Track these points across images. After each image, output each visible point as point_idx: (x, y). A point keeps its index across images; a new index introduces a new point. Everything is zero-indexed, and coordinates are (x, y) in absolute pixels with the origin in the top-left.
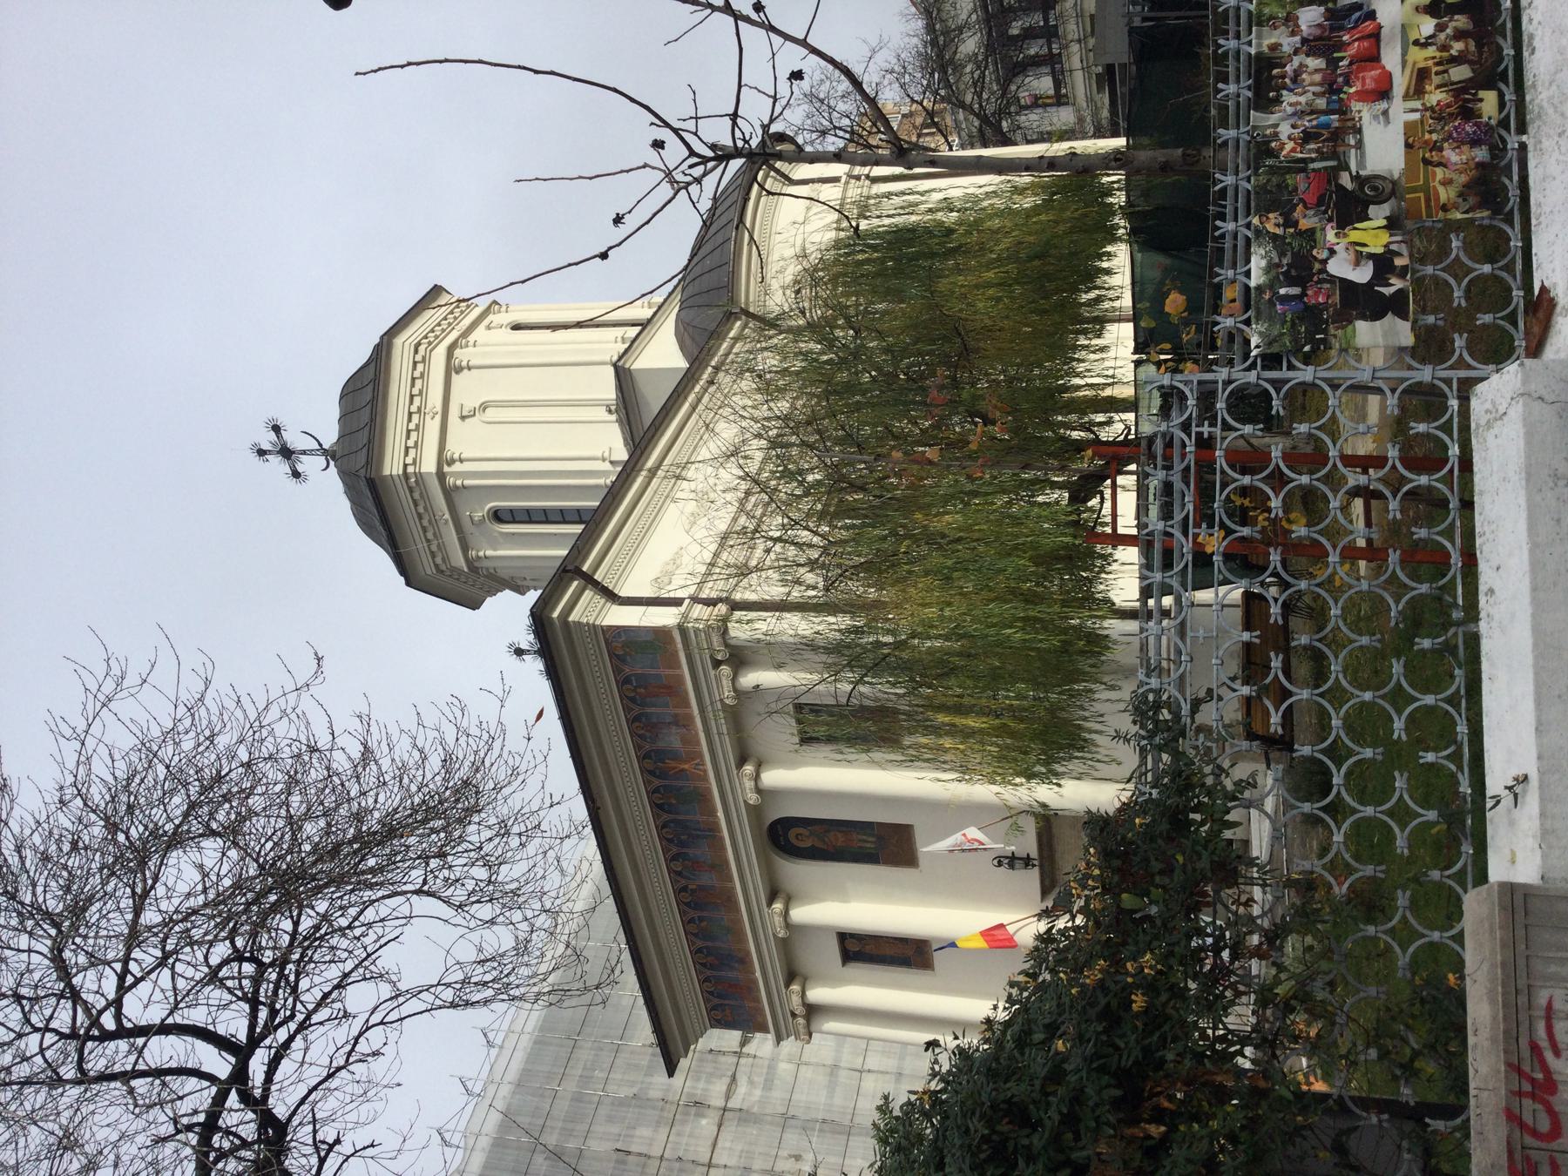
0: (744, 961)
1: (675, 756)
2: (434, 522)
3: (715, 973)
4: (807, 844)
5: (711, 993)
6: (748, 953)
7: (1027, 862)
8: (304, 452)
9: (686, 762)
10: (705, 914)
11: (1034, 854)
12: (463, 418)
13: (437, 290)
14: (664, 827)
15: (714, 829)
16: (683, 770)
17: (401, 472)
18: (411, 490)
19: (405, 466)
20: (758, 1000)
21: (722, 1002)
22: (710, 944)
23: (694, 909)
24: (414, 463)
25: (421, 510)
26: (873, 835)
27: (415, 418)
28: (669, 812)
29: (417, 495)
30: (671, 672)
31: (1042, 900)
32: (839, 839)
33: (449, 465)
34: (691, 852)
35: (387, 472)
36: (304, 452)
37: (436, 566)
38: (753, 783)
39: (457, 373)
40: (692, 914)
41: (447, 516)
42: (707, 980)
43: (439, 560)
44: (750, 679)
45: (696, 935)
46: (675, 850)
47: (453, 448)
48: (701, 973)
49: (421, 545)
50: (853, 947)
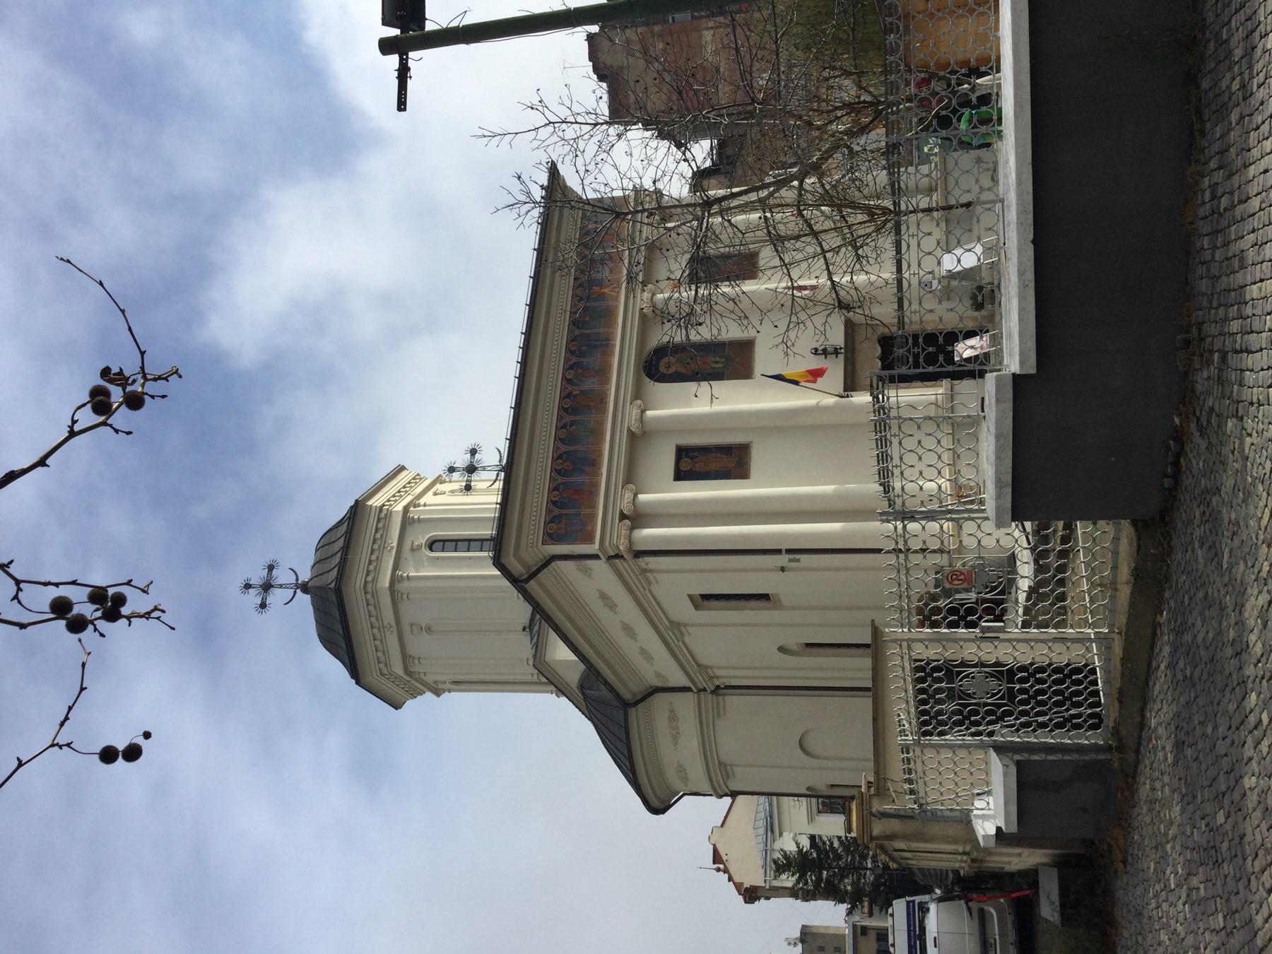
2: (383, 548)
4: (671, 370)
6: (600, 454)
7: (836, 352)
8: (281, 586)
9: (607, 286)
18: (379, 521)
19: (383, 505)
20: (593, 506)
22: (571, 448)
28: (578, 328)
29: (381, 525)
36: (281, 586)
37: (366, 582)
38: (650, 295)
40: (568, 419)
41: (395, 544)
46: (574, 360)
50: (685, 466)
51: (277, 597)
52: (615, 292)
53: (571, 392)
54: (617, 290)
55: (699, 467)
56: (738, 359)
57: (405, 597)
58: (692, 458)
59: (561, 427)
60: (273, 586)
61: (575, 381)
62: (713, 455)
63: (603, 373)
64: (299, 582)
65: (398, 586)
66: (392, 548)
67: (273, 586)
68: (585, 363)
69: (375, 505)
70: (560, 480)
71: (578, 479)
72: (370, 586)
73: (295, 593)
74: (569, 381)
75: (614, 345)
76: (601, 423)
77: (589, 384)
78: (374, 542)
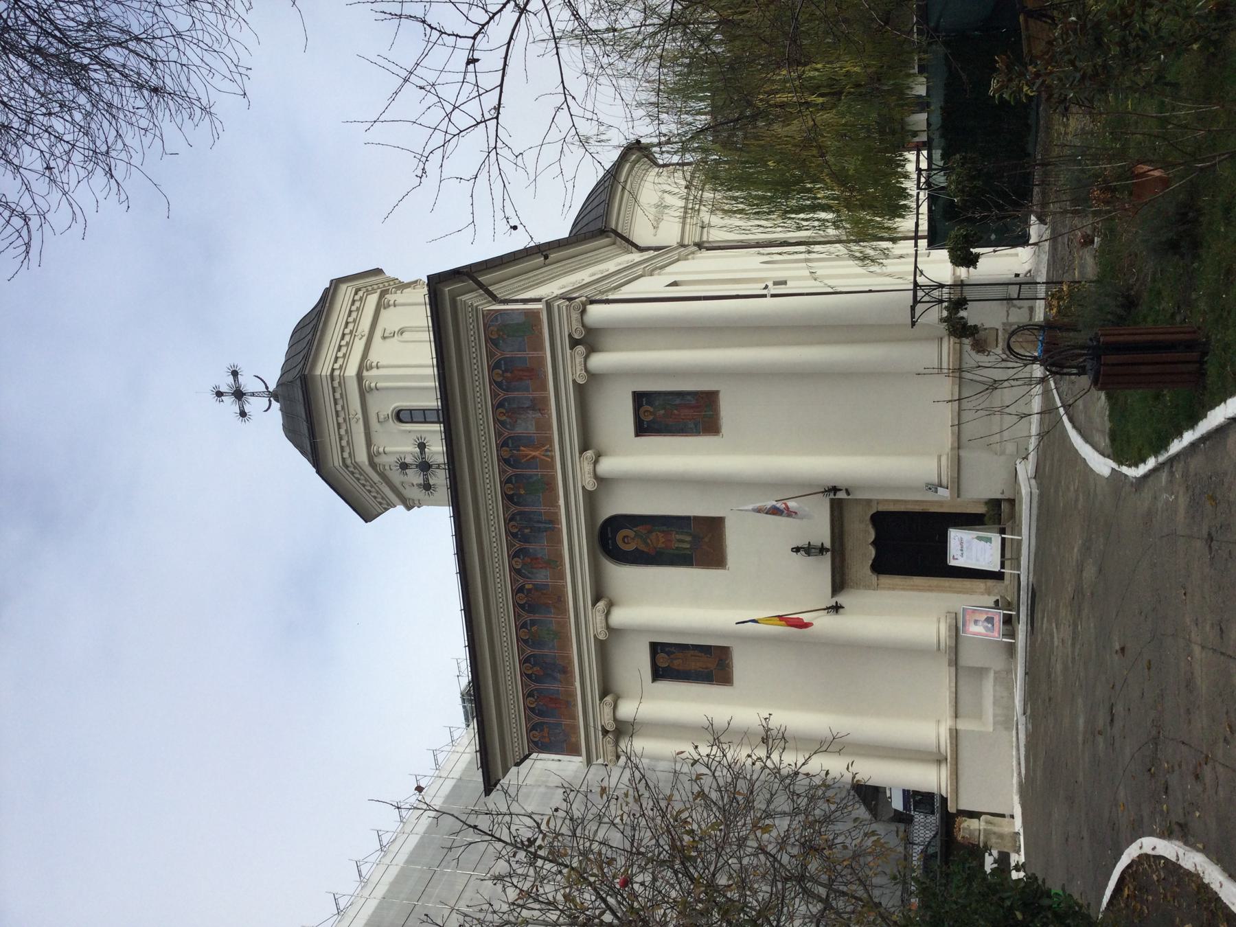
0: (566, 671)
1: (530, 442)
3: (539, 686)
4: (630, 547)
5: (532, 710)
6: (570, 661)
7: (822, 550)
8: (253, 394)
9: (537, 448)
10: (536, 617)
11: (828, 544)
12: (384, 338)
13: (378, 272)
14: (511, 520)
15: (553, 521)
16: (534, 457)
17: (329, 373)
19: (333, 370)
20: (574, 717)
21: (542, 720)
22: (537, 652)
23: (529, 612)
24: (341, 367)
25: (339, 408)
26: (690, 534)
27: (347, 338)
28: (515, 504)
30: (535, 354)
31: (832, 597)
32: (658, 540)
33: (367, 370)
34: (531, 547)
35: (318, 372)
36: (253, 394)
37: (344, 459)
38: (591, 467)
39: (385, 308)
40: (527, 617)
41: (360, 415)
42: (530, 695)
43: (346, 455)
44: (599, 361)
45: (525, 641)
46: (518, 546)
47: (373, 357)
48: (527, 685)
49: (334, 438)
50: (663, 662)
51: (255, 405)
52: (547, 456)
53: (523, 586)
54: (549, 453)
55: (677, 664)
56: (706, 540)
57: (387, 468)
58: (668, 654)
59: (521, 626)
60: (245, 394)
61: (523, 571)
62: (692, 652)
63: (554, 563)
64: (271, 389)
65: (376, 460)
66: (358, 420)
67: (245, 394)
68: (531, 550)
69: (324, 373)
70: (533, 686)
71: (553, 686)
72: (348, 462)
73: (270, 401)
74: (518, 572)
75: (560, 530)
76: (564, 625)
77: (542, 577)
78: (337, 415)
